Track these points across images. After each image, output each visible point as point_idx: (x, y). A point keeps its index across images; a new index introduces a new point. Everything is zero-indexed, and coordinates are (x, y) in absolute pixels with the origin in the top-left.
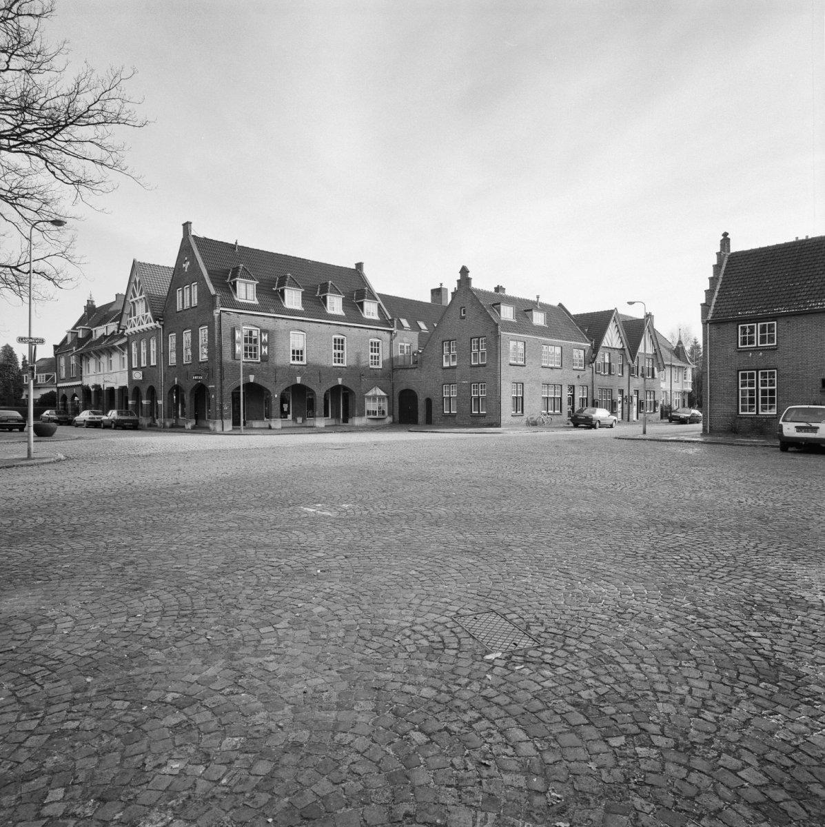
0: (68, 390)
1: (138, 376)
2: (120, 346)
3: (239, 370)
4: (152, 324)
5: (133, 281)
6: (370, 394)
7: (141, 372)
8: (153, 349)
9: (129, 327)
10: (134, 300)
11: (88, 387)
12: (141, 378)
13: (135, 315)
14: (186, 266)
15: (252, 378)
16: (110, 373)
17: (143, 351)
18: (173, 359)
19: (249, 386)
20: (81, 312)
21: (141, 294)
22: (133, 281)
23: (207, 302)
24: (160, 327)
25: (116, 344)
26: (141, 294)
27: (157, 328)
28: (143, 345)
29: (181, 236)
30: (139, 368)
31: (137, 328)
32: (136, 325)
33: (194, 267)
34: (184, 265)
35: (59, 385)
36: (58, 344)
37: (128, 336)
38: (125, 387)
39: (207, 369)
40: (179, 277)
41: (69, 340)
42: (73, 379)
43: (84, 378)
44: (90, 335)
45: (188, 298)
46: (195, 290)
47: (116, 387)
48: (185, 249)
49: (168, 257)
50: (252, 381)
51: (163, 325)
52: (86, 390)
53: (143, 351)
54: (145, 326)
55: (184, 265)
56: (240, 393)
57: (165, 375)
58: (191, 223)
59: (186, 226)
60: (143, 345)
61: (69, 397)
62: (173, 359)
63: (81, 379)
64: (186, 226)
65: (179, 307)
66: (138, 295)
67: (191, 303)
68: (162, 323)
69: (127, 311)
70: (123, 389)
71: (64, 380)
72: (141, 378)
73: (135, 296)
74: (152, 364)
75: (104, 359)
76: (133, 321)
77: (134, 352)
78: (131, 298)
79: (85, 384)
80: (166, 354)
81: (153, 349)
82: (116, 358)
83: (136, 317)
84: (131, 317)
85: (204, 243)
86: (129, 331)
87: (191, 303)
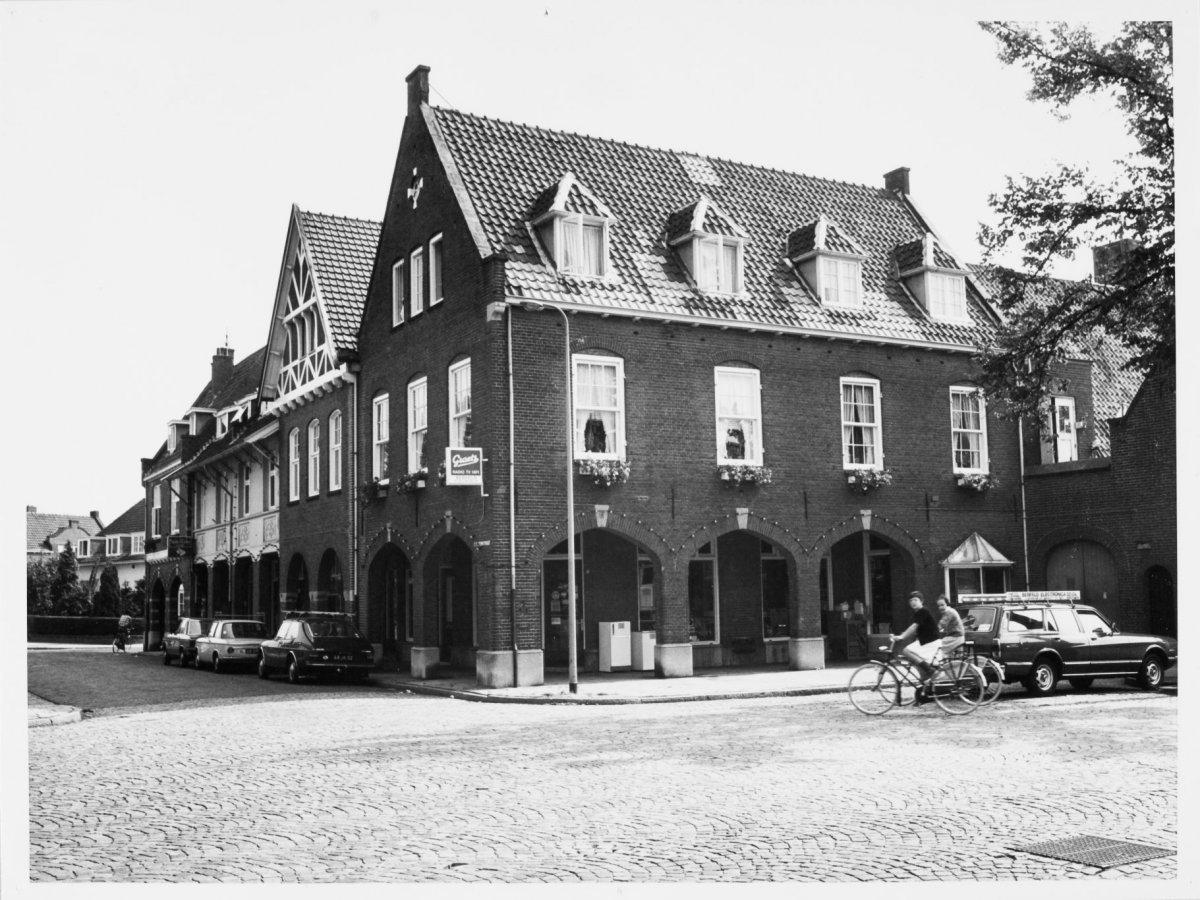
4: (331, 376)
8: (335, 446)
15: (602, 516)
16: (246, 528)
17: (314, 453)
19: (593, 540)
20: (204, 377)
21: (307, 298)
24: (350, 378)
25: (252, 439)
26: (307, 298)
27: (345, 384)
29: (402, 111)
31: (302, 390)
34: (410, 192)
36: (151, 455)
41: (171, 449)
48: (416, 146)
50: (602, 522)
51: (358, 375)
53: (314, 453)
55: (410, 192)
56: (565, 563)
59: (418, 82)
60: (313, 437)
64: (418, 82)
66: (300, 299)
68: (356, 368)
73: (295, 305)
76: (291, 372)
77: (294, 459)
78: (288, 312)
81: (335, 446)
83: (297, 362)
84: (286, 363)
85: (476, 132)
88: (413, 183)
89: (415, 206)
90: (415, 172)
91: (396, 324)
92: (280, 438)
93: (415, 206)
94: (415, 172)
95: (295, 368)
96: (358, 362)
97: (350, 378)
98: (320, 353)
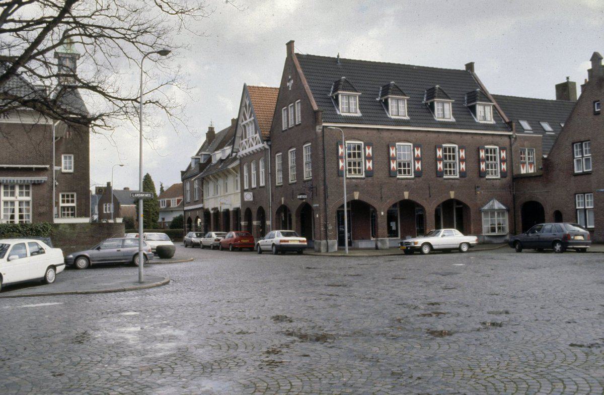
0: (193, 212)
1: (249, 197)
2: (233, 168)
3: (343, 187)
4: (261, 145)
5: (243, 105)
6: (486, 208)
7: (251, 193)
8: (262, 170)
9: (241, 150)
10: (245, 122)
11: (207, 210)
12: (252, 199)
13: (246, 138)
14: (290, 84)
15: (357, 196)
16: (226, 197)
17: (253, 172)
18: (279, 180)
19: (353, 204)
20: (204, 139)
21: (250, 117)
22: (243, 105)
23: (312, 117)
24: (267, 147)
25: (230, 167)
26: (250, 117)
27: (265, 149)
28: (253, 166)
29: (284, 55)
30: (251, 189)
31: (248, 150)
32: (247, 147)
33: (298, 85)
34: (288, 84)
35: (186, 208)
36: (184, 170)
37: (241, 159)
39: (312, 187)
40: (284, 96)
41: (193, 166)
42: (196, 202)
43: (205, 201)
44: (209, 160)
45: (292, 116)
46: (298, 108)
47: (231, 209)
49: (270, 76)
51: (270, 146)
52: (206, 213)
53: (253, 172)
54: (256, 147)
55: (288, 84)
56: (343, 211)
57: (272, 196)
58: (293, 42)
59: (290, 45)
60: (253, 166)
61: (193, 220)
62: (279, 180)
63: (202, 202)
64: (290, 45)
65: (284, 127)
66: (248, 117)
67: (295, 122)
68: (269, 143)
69: (239, 134)
70: (237, 211)
71: (189, 204)
72: (252, 199)
73: (246, 119)
74: (262, 184)
75: (221, 182)
76: (244, 143)
77: (246, 174)
78: (243, 121)
79: (206, 207)
80: (273, 174)
81: (262, 170)
82: (231, 181)
83: (246, 140)
84: (242, 139)
85: (309, 61)
86: (242, 153)
87: (295, 122)
88: (290, 80)
89: (290, 89)
90: (290, 77)
91: (283, 129)
92: (241, 167)
93: (290, 89)
94: (290, 77)
95: (246, 142)
96: (270, 141)
97: (267, 147)
98: (256, 137)
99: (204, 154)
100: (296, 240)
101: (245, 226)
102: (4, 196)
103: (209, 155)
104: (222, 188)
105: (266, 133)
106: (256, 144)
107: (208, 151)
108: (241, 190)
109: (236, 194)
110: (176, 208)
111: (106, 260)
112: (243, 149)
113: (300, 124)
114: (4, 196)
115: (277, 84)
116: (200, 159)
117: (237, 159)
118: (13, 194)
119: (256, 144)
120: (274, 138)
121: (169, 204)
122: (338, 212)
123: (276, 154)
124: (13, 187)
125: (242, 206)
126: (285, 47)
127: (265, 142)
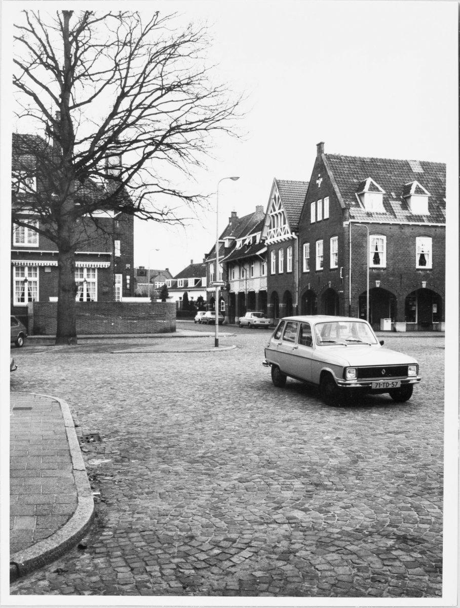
2: (261, 255)
3: (366, 276)
4: (289, 235)
5: (273, 197)
8: (289, 258)
9: (269, 238)
10: (273, 213)
11: (234, 293)
13: (274, 227)
14: (319, 182)
15: (378, 284)
17: (281, 259)
19: (374, 290)
21: (279, 209)
23: (339, 212)
24: (295, 237)
25: (258, 253)
26: (279, 209)
27: (293, 239)
28: (281, 253)
31: (276, 239)
32: (275, 236)
33: (327, 183)
37: (268, 246)
38: (265, 291)
40: (313, 193)
45: (320, 211)
47: (257, 291)
50: (378, 286)
53: (281, 259)
54: (284, 237)
58: (323, 143)
59: (320, 146)
60: (281, 253)
64: (320, 146)
65: (313, 220)
66: (277, 208)
67: (323, 216)
68: (298, 234)
69: (267, 224)
70: (262, 293)
73: (275, 210)
74: (289, 270)
75: (247, 267)
76: (272, 232)
77: (273, 260)
78: (271, 212)
81: (289, 258)
82: (257, 268)
83: (275, 229)
84: (270, 228)
87: (323, 216)
88: (318, 178)
89: (319, 186)
90: (319, 175)
93: (319, 186)
94: (319, 175)
95: (274, 231)
97: (295, 237)
98: (284, 228)
99: (229, 239)
100: (267, 321)
101: (270, 308)
102: (16, 276)
103: (234, 239)
104: (248, 273)
105: (295, 224)
106: (285, 234)
107: (232, 236)
108: (268, 274)
109: (261, 278)
110: (194, 288)
111: (150, 337)
112: (271, 238)
113: (327, 219)
114: (16, 276)
115: (307, 178)
116: (224, 243)
117: (265, 246)
118: (23, 275)
119: (285, 234)
120: (304, 229)
121: (186, 284)
122: (360, 298)
123: (304, 243)
124: (23, 268)
125: (268, 289)
126: (316, 148)
127: (293, 233)
